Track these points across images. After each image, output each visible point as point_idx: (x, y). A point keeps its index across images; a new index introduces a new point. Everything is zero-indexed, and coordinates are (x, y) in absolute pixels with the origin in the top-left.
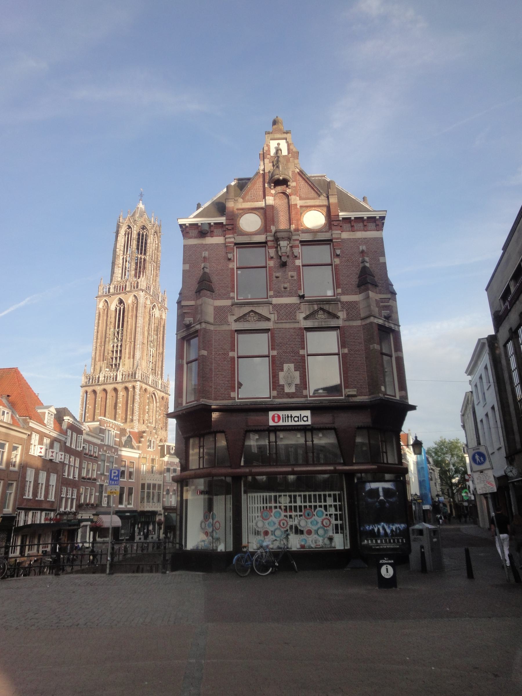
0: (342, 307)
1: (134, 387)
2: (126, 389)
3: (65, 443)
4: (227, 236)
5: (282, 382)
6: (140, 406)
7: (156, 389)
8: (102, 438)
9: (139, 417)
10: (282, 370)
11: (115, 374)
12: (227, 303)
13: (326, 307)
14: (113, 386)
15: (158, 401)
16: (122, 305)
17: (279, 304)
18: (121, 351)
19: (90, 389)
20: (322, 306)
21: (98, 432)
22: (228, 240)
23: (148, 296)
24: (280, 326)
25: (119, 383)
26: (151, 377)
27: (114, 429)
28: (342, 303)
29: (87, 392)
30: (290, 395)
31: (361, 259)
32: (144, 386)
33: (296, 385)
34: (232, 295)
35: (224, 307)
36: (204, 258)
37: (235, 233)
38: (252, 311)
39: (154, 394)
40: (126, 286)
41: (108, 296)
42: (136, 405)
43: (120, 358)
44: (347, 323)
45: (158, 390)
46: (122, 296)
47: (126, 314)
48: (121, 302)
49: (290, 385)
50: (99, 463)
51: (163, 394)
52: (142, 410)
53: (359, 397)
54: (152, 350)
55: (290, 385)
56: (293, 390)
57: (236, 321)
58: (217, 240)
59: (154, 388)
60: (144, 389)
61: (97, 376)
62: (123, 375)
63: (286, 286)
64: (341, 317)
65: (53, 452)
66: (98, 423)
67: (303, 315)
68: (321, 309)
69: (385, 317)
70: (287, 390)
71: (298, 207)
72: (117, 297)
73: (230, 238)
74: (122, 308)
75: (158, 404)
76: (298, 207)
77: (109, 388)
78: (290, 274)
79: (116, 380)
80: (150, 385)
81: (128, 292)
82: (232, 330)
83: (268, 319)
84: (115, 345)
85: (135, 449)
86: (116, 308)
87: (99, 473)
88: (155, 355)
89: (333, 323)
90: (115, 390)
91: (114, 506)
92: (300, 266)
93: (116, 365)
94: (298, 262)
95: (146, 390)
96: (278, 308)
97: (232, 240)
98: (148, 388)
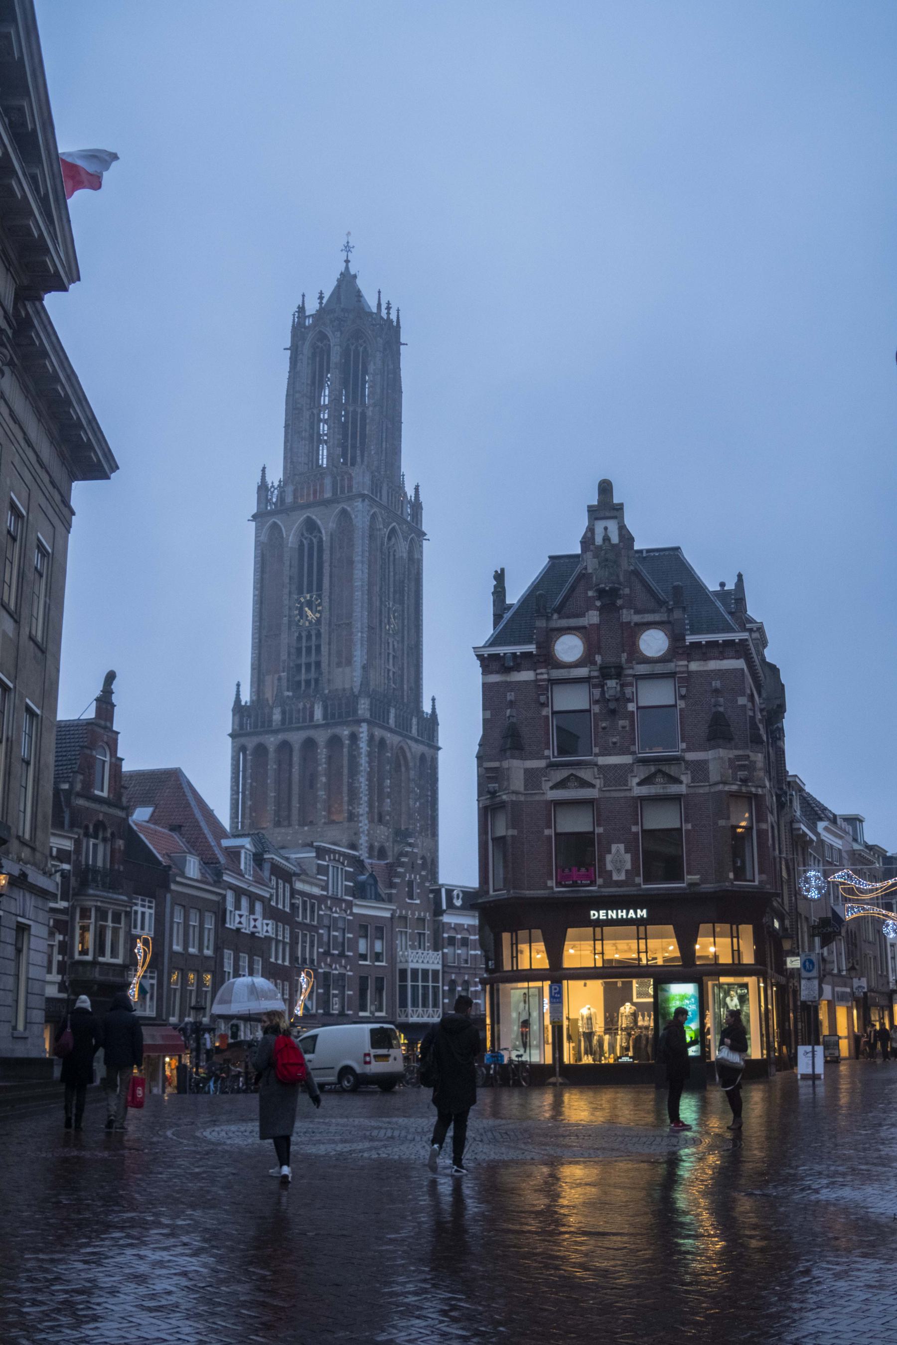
0: (687, 769)
1: (354, 737)
3: (270, 899)
4: (539, 671)
5: (609, 867)
6: (370, 780)
8: (323, 884)
9: (370, 805)
10: (609, 852)
12: (542, 764)
13: (665, 768)
15: (411, 764)
17: (607, 766)
18: (318, 647)
19: (251, 743)
20: (660, 767)
21: (315, 871)
22: (539, 677)
23: (375, 509)
24: (607, 795)
27: (343, 864)
28: (686, 762)
29: (243, 749)
30: (618, 884)
31: (713, 700)
32: (378, 733)
33: (627, 871)
34: (546, 753)
35: (537, 769)
36: (511, 701)
37: (549, 665)
38: (572, 775)
39: (402, 748)
42: (363, 781)
43: (318, 664)
44: (692, 791)
45: (412, 738)
46: (314, 514)
47: (326, 556)
49: (619, 871)
50: (321, 931)
52: (377, 791)
53: (703, 886)
54: (390, 641)
55: (619, 871)
56: (622, 877)
57: (552, 788)
58: (526, 676)
59: (400, 734)
60: (377, 739)
63: (614, 740)
64: (685, 782)
65: (241, 916)
66: (314, 854)
67: (637, 780)
68: (660, 771)
69: (741, 780)
70: (615, 877)
71: (632, 624)
72: (300, 518)
73: (542, 674)
75: (412, 773)
76: (632, 624)
77: (296, 738)
78: (621, 723)
80: (391, 730)
82: (547, 801)
83: (593, 786)
84: (304, 634)
85: (383, 900)
87: (321, 950)
89: (674, 789)
90: (310, 744)
91: (350, 1012)
92: (633, 712)
93: (308, 682)
94: (631, 707)
95: (382, 742)
96: (604, 770)
97: (545, 676)
98: (388, 735)
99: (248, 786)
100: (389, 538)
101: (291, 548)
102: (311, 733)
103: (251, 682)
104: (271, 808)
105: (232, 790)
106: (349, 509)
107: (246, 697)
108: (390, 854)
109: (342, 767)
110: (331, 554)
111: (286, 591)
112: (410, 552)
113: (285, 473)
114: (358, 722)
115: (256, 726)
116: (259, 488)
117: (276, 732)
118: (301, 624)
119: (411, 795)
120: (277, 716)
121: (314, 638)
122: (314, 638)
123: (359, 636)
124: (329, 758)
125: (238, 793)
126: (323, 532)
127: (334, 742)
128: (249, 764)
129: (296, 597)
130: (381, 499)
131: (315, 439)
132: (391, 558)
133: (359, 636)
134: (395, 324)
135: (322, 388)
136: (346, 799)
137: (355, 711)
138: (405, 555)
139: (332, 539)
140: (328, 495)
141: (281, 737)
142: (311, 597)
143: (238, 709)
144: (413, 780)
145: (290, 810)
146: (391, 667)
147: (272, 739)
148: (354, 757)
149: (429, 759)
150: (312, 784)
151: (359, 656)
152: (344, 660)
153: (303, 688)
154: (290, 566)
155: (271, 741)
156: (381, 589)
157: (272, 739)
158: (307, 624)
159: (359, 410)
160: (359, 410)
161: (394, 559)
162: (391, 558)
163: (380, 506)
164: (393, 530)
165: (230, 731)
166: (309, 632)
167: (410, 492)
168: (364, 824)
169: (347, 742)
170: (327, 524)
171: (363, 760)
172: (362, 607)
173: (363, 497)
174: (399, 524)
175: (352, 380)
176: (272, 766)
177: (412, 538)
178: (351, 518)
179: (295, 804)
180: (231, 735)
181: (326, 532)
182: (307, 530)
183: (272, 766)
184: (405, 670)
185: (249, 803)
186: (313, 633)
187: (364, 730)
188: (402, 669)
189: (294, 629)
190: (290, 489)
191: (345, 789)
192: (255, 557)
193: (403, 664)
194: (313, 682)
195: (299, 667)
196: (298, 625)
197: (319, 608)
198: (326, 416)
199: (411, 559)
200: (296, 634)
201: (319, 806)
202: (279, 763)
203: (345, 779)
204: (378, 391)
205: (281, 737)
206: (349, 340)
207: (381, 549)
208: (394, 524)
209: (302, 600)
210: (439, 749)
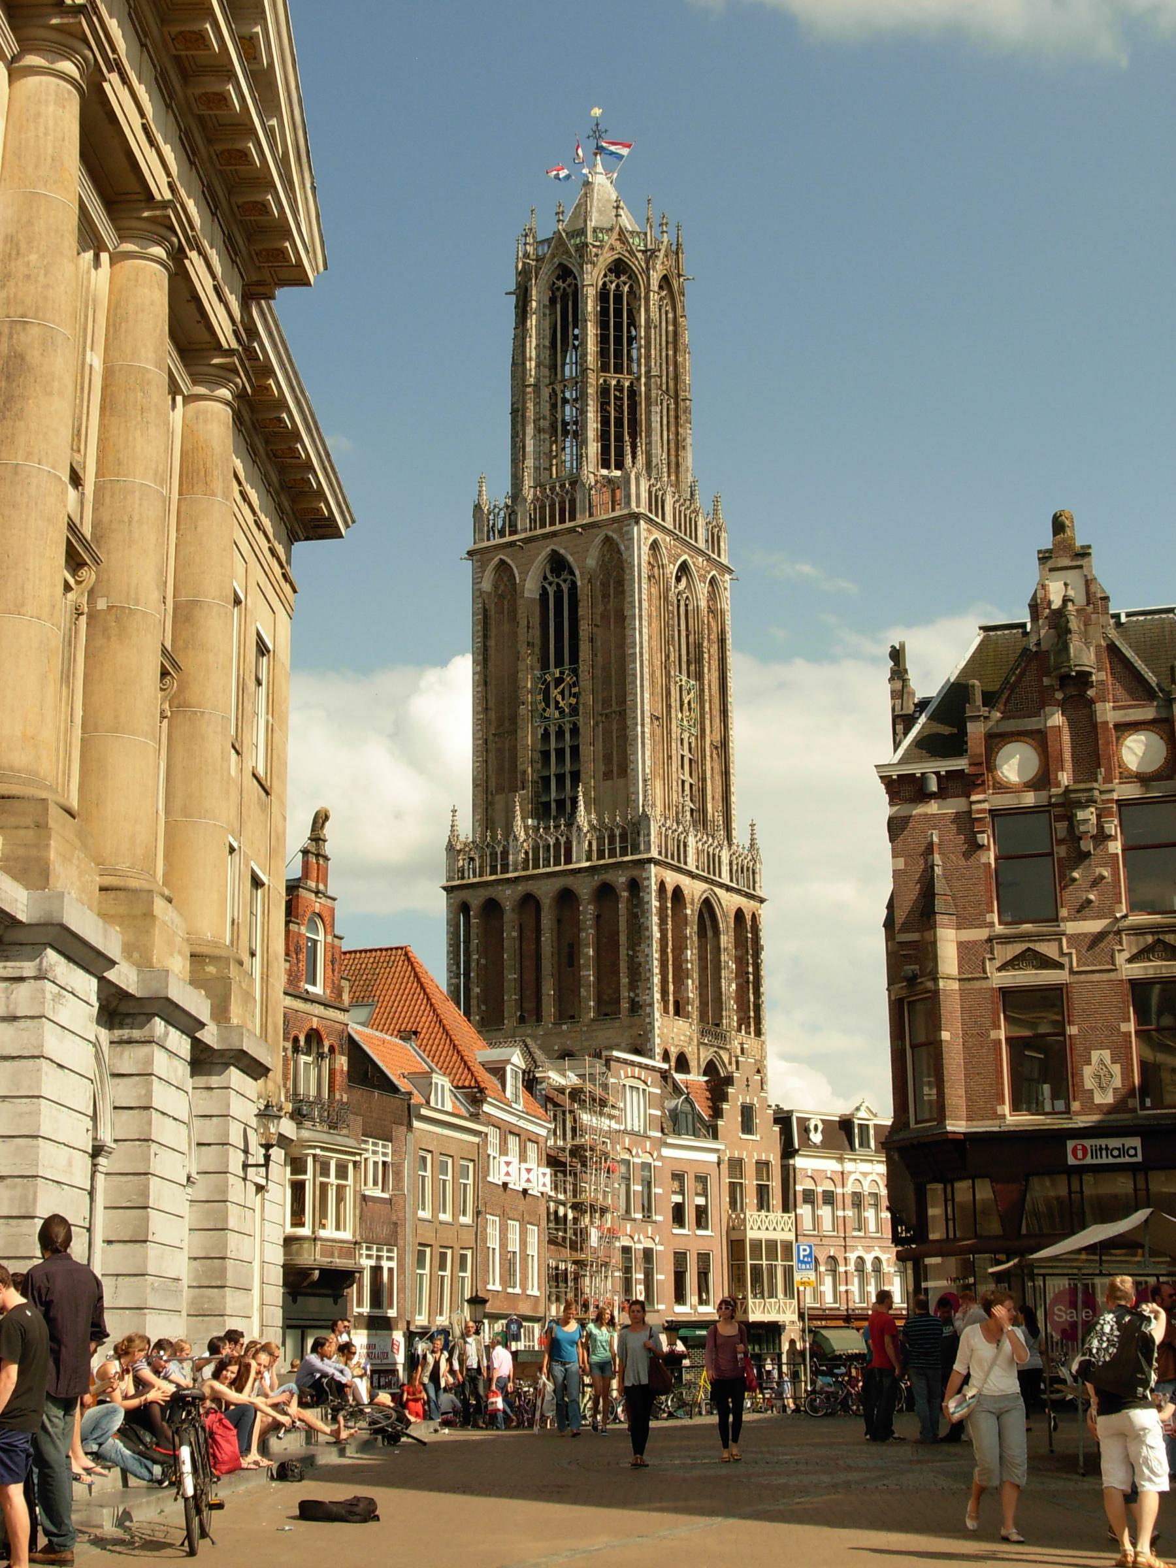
2: (605, 892)
6: (663, 952)
7: (712, 882)
11: (563, 840)
14: (559, 883)
16: (565, 575)
18: (575, 750)
19: (476, 900)
23: (657, 535)
26: (691, 841)
29: (465, 908)
32: (672, 879)
40: (573, 502)
45: (721, 886)
48: (558, 564)
54: (686, 735)
60: (670, 888)
61: (499, 850)
74: (565, 587)
77: (546, 892)
84: (553, 730)
90: (566, 898)
93: (561, 804)
95: (678, 891)
98: (685, 882)
100: (678, 579)
102: (569, 881)
103: (474, 805)
104: (511, 998)
105: (449, 971)
106: (615, 536)
108: (693, 1064)
109: (618, 933)
118: (546, 715)
121: (568, 735)
122: (568, 735)
124: (598, 917)
125: (458, 976)
126: (577, 573)
127: (605, 892)
129: (537, 673)
130: (663, 519)
132: (682, 609)
136: (624, 980)
138: (703, 604)
141: (521, 888)
142: (562, 673)
144: (726, 949)
146: (687, 777)
147: (508, 892)
148: (636, 916)
149: (748, 917)
152: (615, 769)
153: (553, 813)
154: (528, 627)
155: (508, 897)
156: (668, 657)
157: (508, 892)
158: (557, 713)
161: (687, 611)
162: (682, 609)
163: (664, 529)
164: (684, 568)
166: (560, 727)
169: (625, 894)
174: (692, 557)
176: (510, 934)
177: (713, 578)
178: (619, 552)
180: (445, 888)
181: (582, 574)
182: (552, 572)
183: (510, 934)
184: (709, 781)
185: (477, 990)
188: (704, 780)
193: (704, 772)
195: (546, 780)
197: (574, 690)
201: (583, 992)
203: (623, 951)
205: (521, 888)
206: (605, 276)
207: (666, 598)
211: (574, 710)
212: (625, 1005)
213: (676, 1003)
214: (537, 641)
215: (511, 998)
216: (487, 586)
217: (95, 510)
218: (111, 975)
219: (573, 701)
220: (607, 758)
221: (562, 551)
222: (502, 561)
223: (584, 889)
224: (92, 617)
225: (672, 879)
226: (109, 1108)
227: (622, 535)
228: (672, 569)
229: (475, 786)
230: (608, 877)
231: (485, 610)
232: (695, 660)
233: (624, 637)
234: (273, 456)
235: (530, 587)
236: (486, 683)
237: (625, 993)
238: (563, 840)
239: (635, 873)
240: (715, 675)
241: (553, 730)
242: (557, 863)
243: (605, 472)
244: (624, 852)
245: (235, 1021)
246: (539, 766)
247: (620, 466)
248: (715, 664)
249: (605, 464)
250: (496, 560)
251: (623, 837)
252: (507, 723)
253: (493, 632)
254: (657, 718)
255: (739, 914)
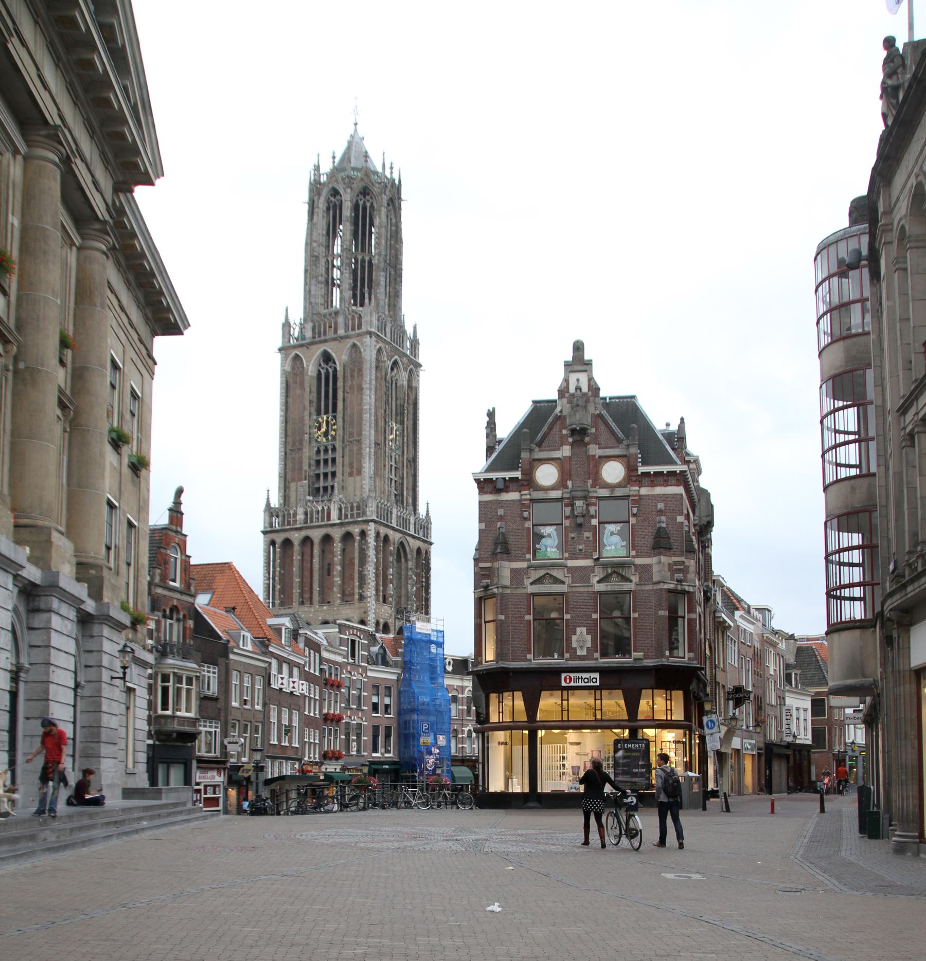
1: (363, 534)
2: (348, 537)
6: (377, 569)
9: (377, 590)
11: (326, 508)
14: (323, 531)
15: (409, 556)
16: (331, 364)
18: (334, 460)
23: (381, 344)
25: (334, 525)
26: (394, 511)
29: (273, 543)
32: (383, 531)
39: (402, 543)
40: (336, 323)
41: (302, 346)
42: (370, 570)
45: (410, 535)
47: (340, 384)
48: (327, 358)
51: (418, 544)
52: (383, 579)
54: (393, 454)
59: (401, 532)
60: (382, 536)
61: (292, 512)
62: (340, 510)
74: (331, 370)
75: (410, 564)
77: (316, 535)
79: (329, 518)
80: (393, 529)
81: (342, 338)
84: (322, 449)
86: (319, 371)
88: (400, 465)
90: (327, 539)
93: (325, 489)
95: (386, 538)
98: (391, 533)
99: (277, 573)
100: (392, 369)
101: (311, 377)
104: (296, 591)
107: (275, 502)
109: (354, 558)
110: (344, 382)
111: (307, 413)
112: (409, 381)
113: (305, 313)
114: (367, 522)
115: (283, 525)
116: (284, 325)
117: (300, 529)
119: (410, 581)
120: (300, 517)
122: (330, 452)
123: (368, 450)
124: (344, 550)
126: (337, 363)
127: (348, 537)
128: (278, 555)
129: (315, 417)
131: (329, 283)
133: (368, 450)
134: (397, 182)
135: (335, 236)
136: (357, 584)
137: (364, 513)
138: (405, 383)
139: (344, 369)
140: (341, 332)
141: (304, 533)
143: (269, 509)
145: (311, 593)
146: (393, 477)
149: (424, 552)
150: (329, 573)
151: (368, 466)
152: (355, 471)
155: (296, 537)
158: (324, 440)
159: (367, 259)
160: (367, 259)
164: (395, 363)
165: (262, 529)
167: (409, 331)
168: (371, 603)
170: (341, 356)
171: (371, 553)
172: (370, 426)
173: (370, 333)
175: (361, 233)
176: (297, 557)
179: (316, 588)
180: (263, 532)
183: (297, 557)
186: (330, 448)
187: (371, 529)
189: (314, 444)
190: (309, 326)
191: (356, 576)
192: (282, 383)
194: (329, 489)
195: (318, 476)
196: (317, 441)
197: (334, 427)
198: (339, 264)
199: (410, 387)
200: (316, 449)
202: (303, 554)
203: (356, 568)
204: (383, 242)
205: (304, 533)
208: (396, 357)
209: (320, 420)
210: (431, 544)
211: (334, 438)
212: (357, 597)
213: (384, 597)
214: (315, 400)
215: (296, 591)
216: (288, 368)
217: (17, 311)
218: (24, 573)
219: (333, 433)
220: (351, 465)
221: (329, 351)
222: (297, 356)
223: (337, 534)
224: (16, 372)
225: (383, 531)
226: (26, 646)
227: (362, 344)
228: (390, 363)
229: (280, 477)
230: (350, 528)
231: (287, 382)
232: (400, 413)
233: (362, 399)
234: (140, 285)
235: (311, 369)
236: (286, 422)
237: (356, 591)
238: (326, 508)
239: (364, 527)
240: (411, 422)
241: (322, 449)
242: (323, 520)
243: (354, 308)
244: (358, 515)
245: (106, 600)
246: (314, 468)
247: (362, 305)
248: (411, 417)
249: (355, 304)
250: (293, 355)
251: (358, 508)
252: (297, 444)
253: (291, 393)
254: (378, 444)
255: (419, 551)
